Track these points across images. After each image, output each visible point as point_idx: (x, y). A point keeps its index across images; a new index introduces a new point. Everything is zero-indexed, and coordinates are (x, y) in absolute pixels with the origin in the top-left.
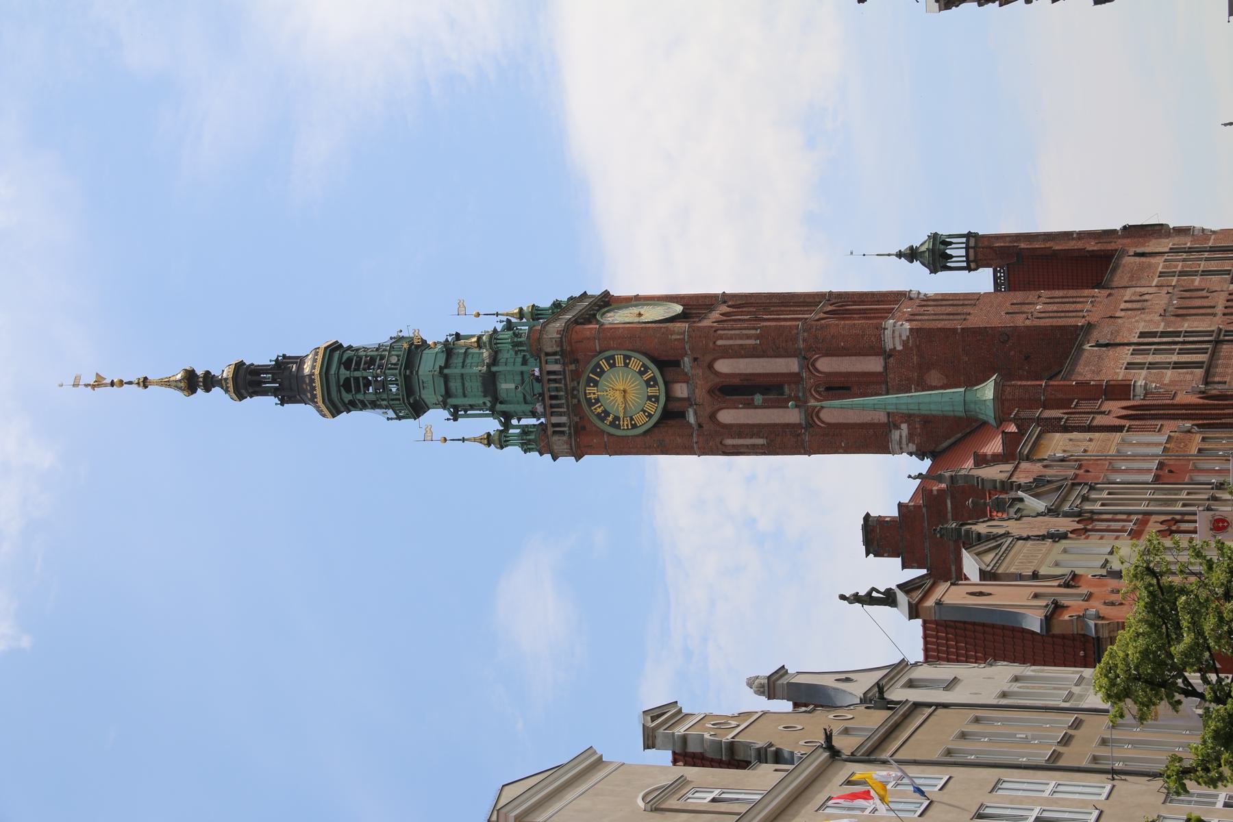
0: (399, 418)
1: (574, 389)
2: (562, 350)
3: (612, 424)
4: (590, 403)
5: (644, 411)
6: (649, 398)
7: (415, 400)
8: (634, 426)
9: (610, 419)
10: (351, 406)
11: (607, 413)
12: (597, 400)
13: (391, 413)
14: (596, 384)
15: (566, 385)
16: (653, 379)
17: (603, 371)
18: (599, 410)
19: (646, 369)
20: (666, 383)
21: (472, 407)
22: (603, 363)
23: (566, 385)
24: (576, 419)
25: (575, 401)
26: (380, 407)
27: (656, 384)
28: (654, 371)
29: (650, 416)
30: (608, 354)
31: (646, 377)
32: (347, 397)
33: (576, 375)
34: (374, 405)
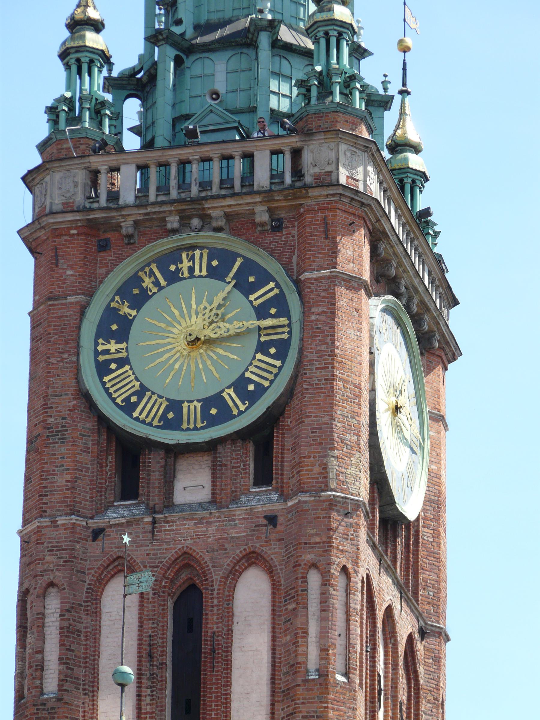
1: (205, 218)
2: (306, 187)
3: (111, 314)
5: (142, 392)
6: (175, 406)
9: (125, 310)
11: (140, 300)
12: (173, 278)
14: (215, 274)
16: (226, 414)
18: (147, 283)
19: (251, 398)
20: (211, 447)
22: (268, 291)
29: (128, 407)
30: (293, 301)
31: (230, 395)
33: (239, 224)
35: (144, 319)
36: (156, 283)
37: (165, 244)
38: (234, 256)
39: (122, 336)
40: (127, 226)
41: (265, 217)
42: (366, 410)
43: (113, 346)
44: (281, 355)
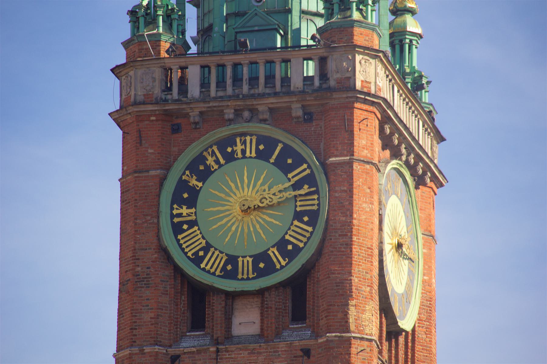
1: (253, 111)
3: (182, 185)
4: (225, 144)
6: (232, 260)
8: (177, 229)
15: (262, 96)
16: (271, 269)
17: (286, 169)
18: (210, 161)
19: (290, 255)
20: (261, 293)
23: (262, 96)
24: (194, 115)
25: (229, 114)
27: (261, 274)
28: (287, 270)
30: (321, 178)
31: (274, 253)
33: (278, 116)
35: (208, 190)
36: (217, 162)
37: (223, 132)
38: (276, 142)
39: (192, 203)
40: (194, 115)
41: (300, 113)
42: (376, 264)
43: (185, 211)
44: (312, 223)
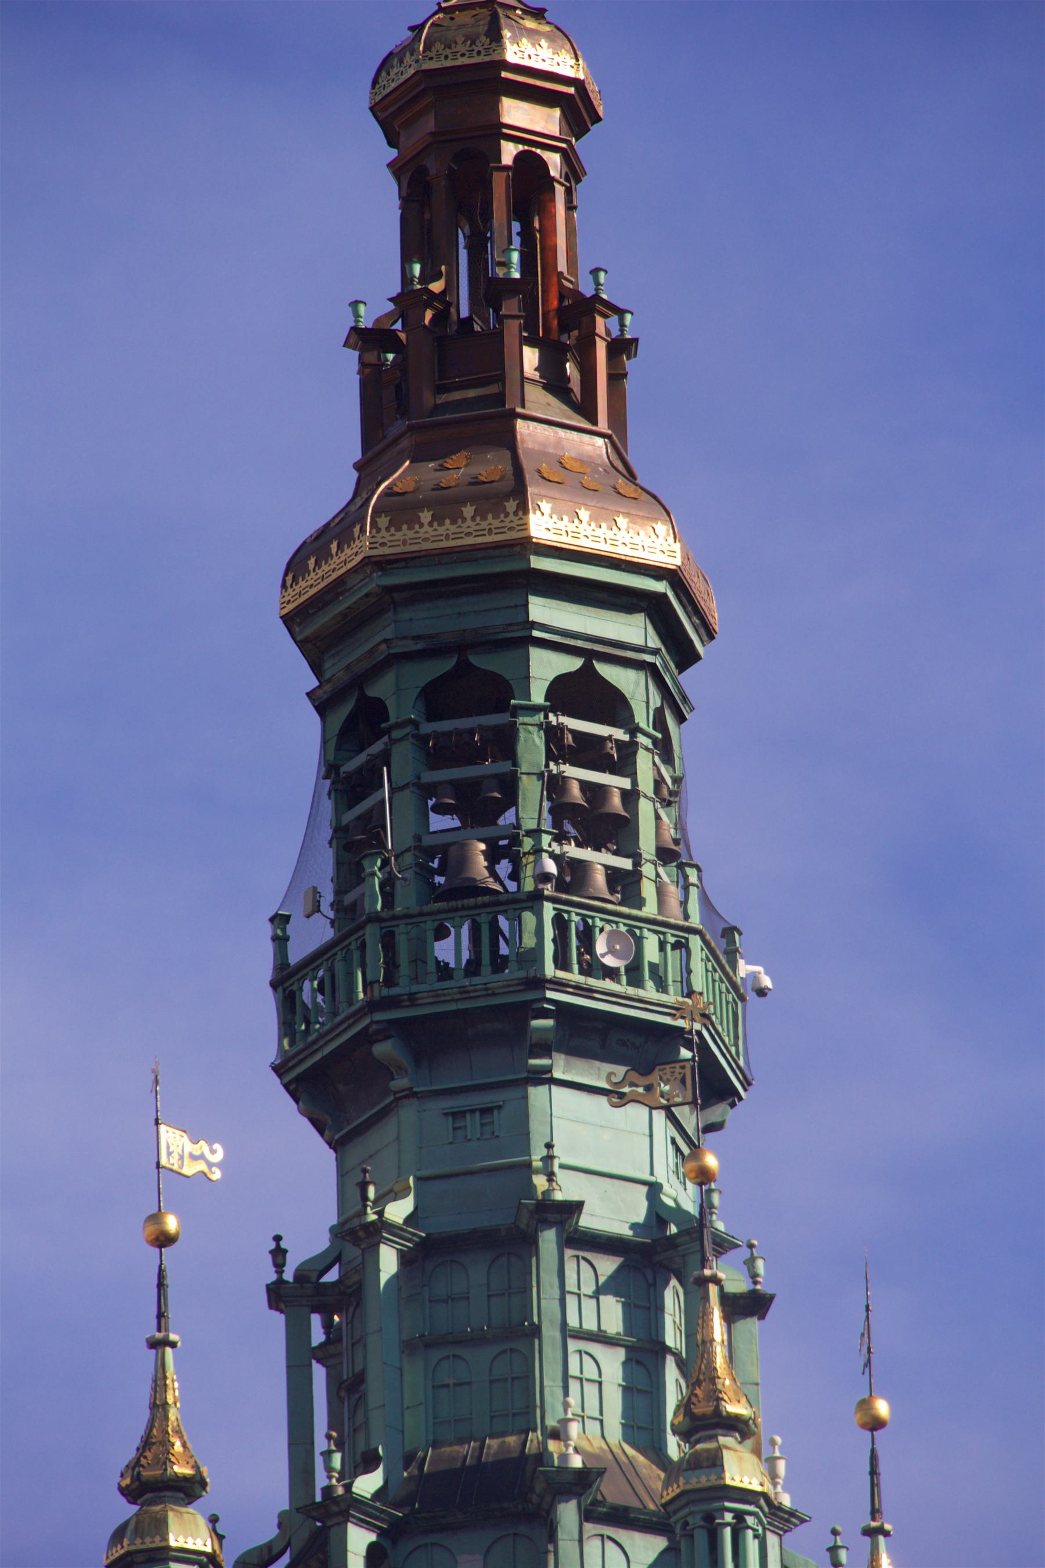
0: (285, 980)
7: (386, 1070)
10: (353, 721)
13: (312, 934)
21: (348, 1390)
26: (349, 873)
32: (398, 694)
34: (354, 842)
